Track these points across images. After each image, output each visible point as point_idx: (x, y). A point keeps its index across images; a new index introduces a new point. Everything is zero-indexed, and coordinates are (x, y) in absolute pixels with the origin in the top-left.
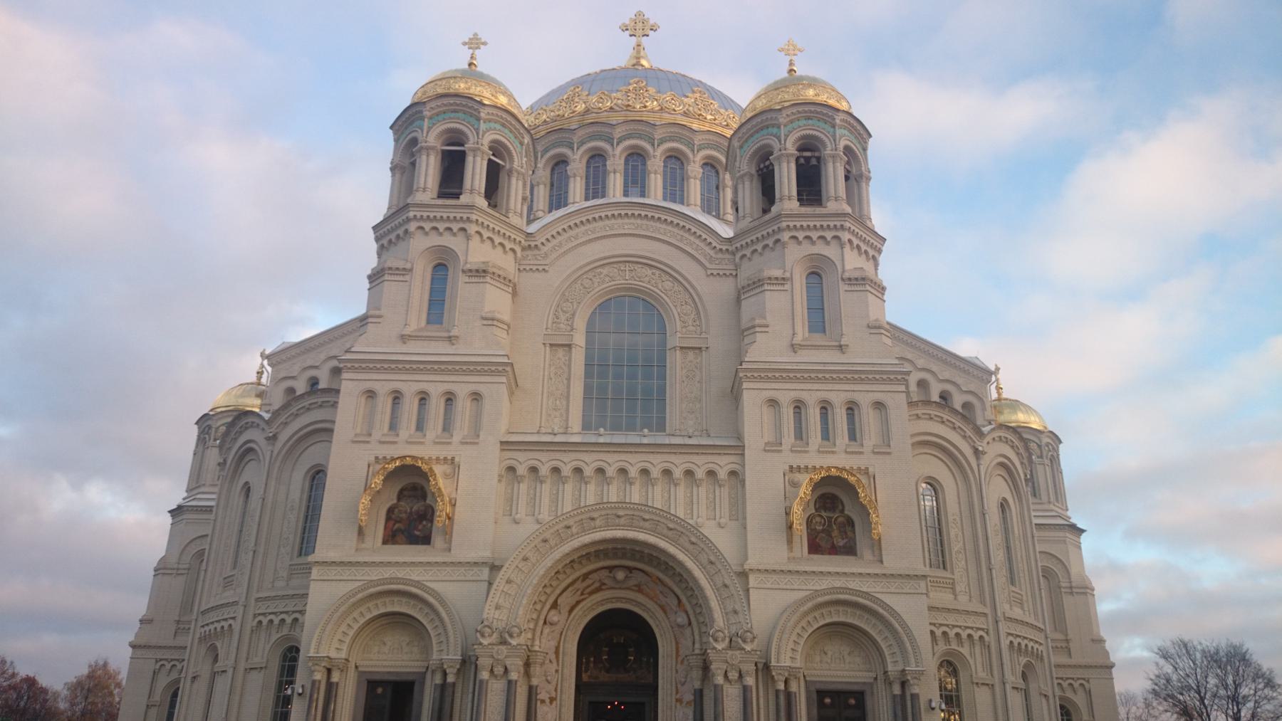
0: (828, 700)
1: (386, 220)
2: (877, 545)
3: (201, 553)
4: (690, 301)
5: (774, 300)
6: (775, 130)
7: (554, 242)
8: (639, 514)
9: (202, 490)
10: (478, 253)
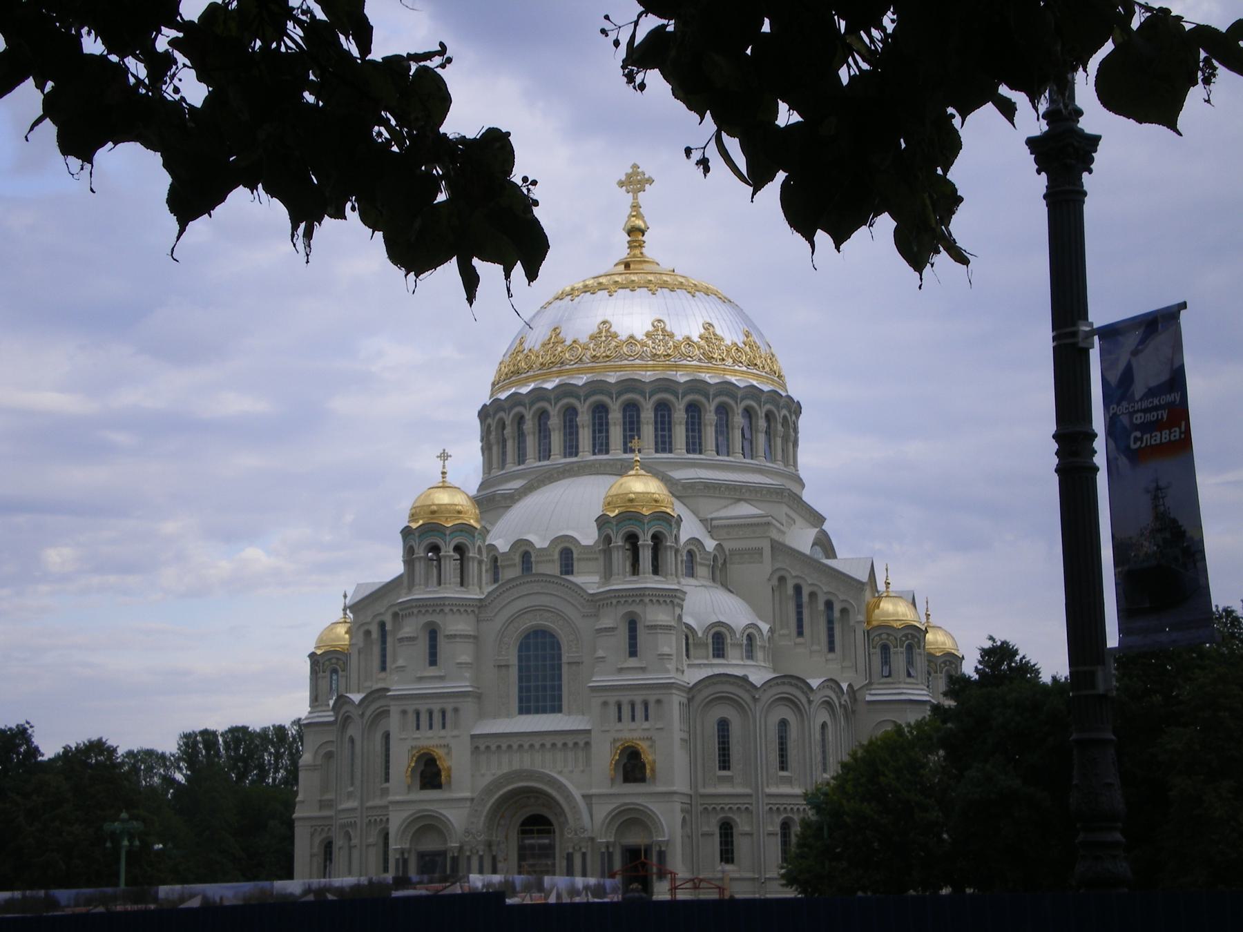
3: (329, 756)
8: (531, 775)
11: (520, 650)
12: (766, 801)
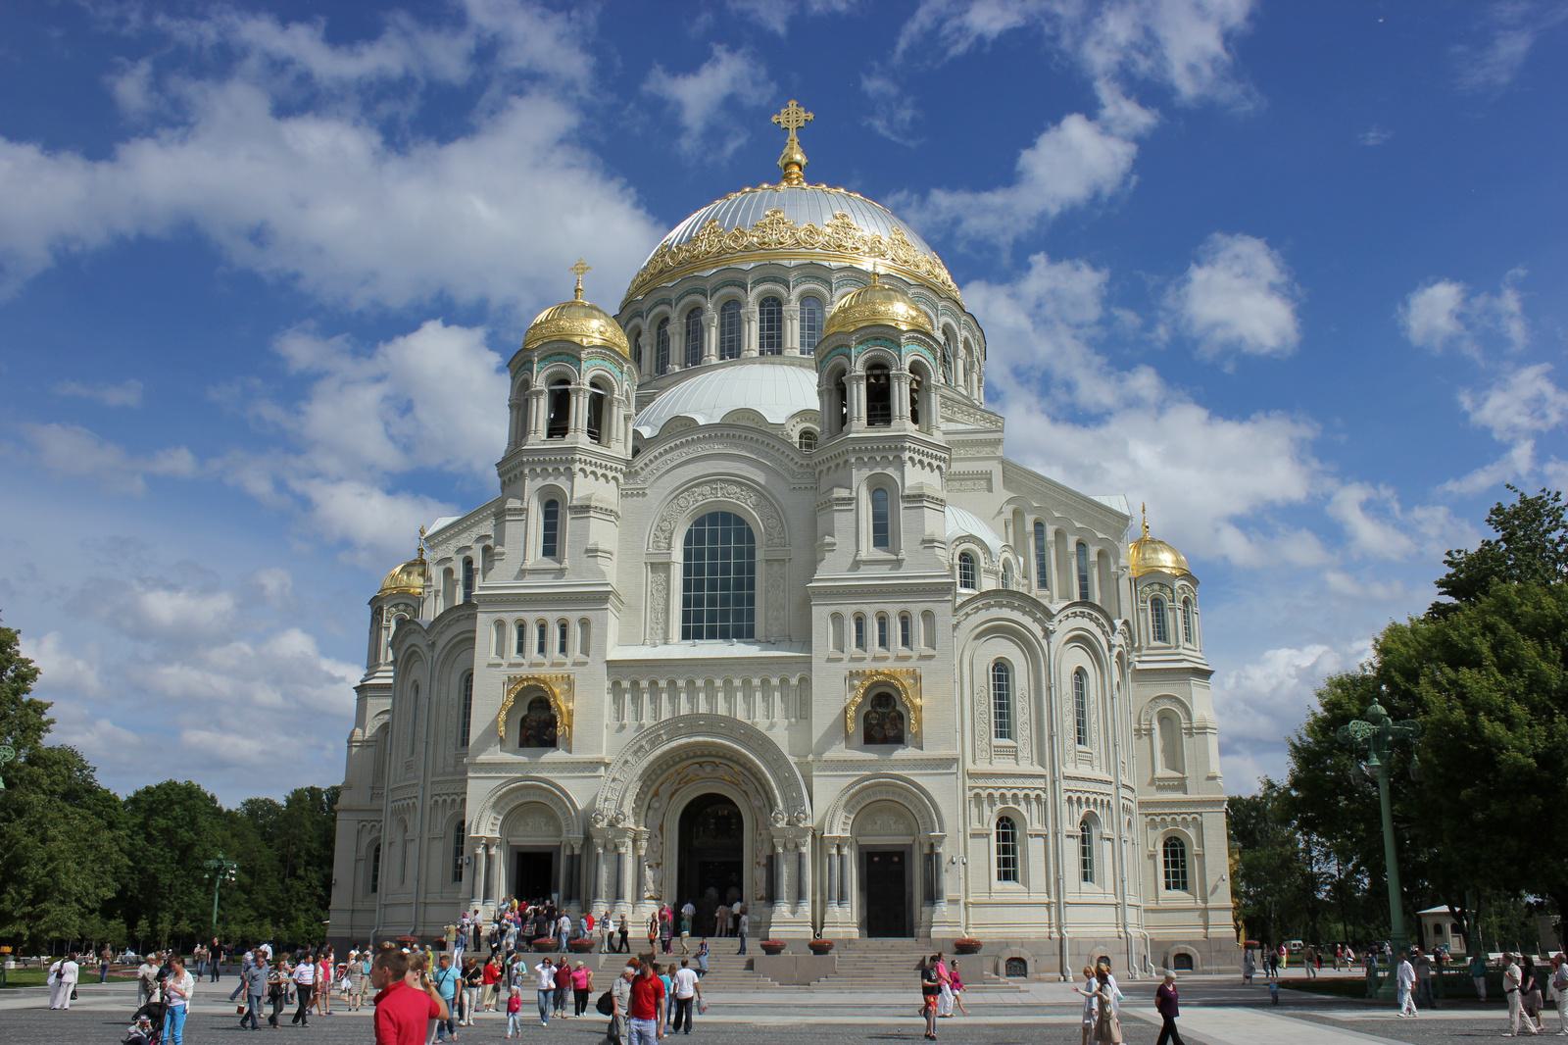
0: (876, 859)
1: (504, 460)
2: (919, 735)
4: (774, 514)
5: (842, 520)
6: (847, 351)
7: (653, 466)
8: (713, 723)
9: (377, 675)
10: (582, 488)
11: (688, 541)
12: (1063, 787)
